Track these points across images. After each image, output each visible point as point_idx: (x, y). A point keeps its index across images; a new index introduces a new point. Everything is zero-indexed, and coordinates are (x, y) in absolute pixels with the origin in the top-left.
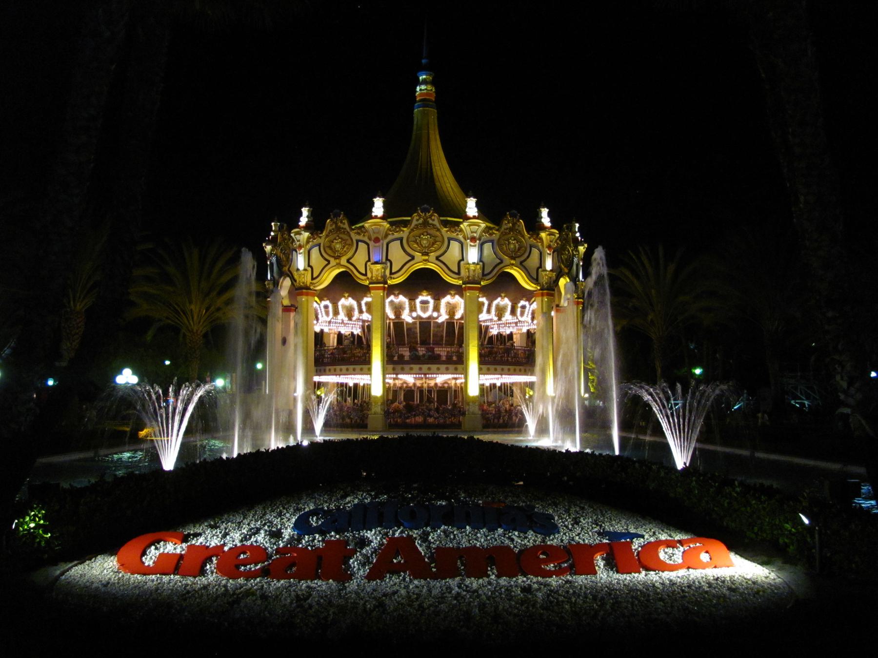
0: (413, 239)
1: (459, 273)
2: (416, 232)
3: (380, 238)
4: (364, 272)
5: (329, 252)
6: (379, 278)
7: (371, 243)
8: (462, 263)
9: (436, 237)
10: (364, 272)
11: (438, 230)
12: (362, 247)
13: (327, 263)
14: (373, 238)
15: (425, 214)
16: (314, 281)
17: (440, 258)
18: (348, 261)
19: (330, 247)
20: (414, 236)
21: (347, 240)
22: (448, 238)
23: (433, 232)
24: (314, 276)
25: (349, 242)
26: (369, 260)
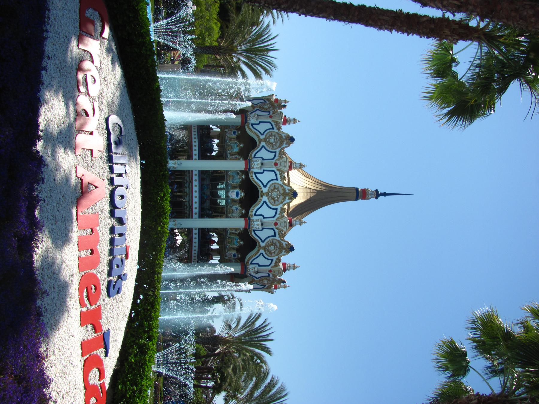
0: (277, 187)
1: (255, 215)
2: (281, 189)
3: (278, 166)
4: (256, 156)
5: (268, 135)
6: (253, 166)
7: (274, 161)
8: (261, 217)
9: (278, 200)
10: (256, 156)
11: (282, 203)
12: (272, 155)
13: (262, 133)
14: (277, 162)
15: (292, 194)
16: (250, 126)
18: (263, 146)
19: (271, 135)
20: (278, 187)
21: (276, 146)
23: (281, 199)
24: (254, 126)
25: (275, 147)
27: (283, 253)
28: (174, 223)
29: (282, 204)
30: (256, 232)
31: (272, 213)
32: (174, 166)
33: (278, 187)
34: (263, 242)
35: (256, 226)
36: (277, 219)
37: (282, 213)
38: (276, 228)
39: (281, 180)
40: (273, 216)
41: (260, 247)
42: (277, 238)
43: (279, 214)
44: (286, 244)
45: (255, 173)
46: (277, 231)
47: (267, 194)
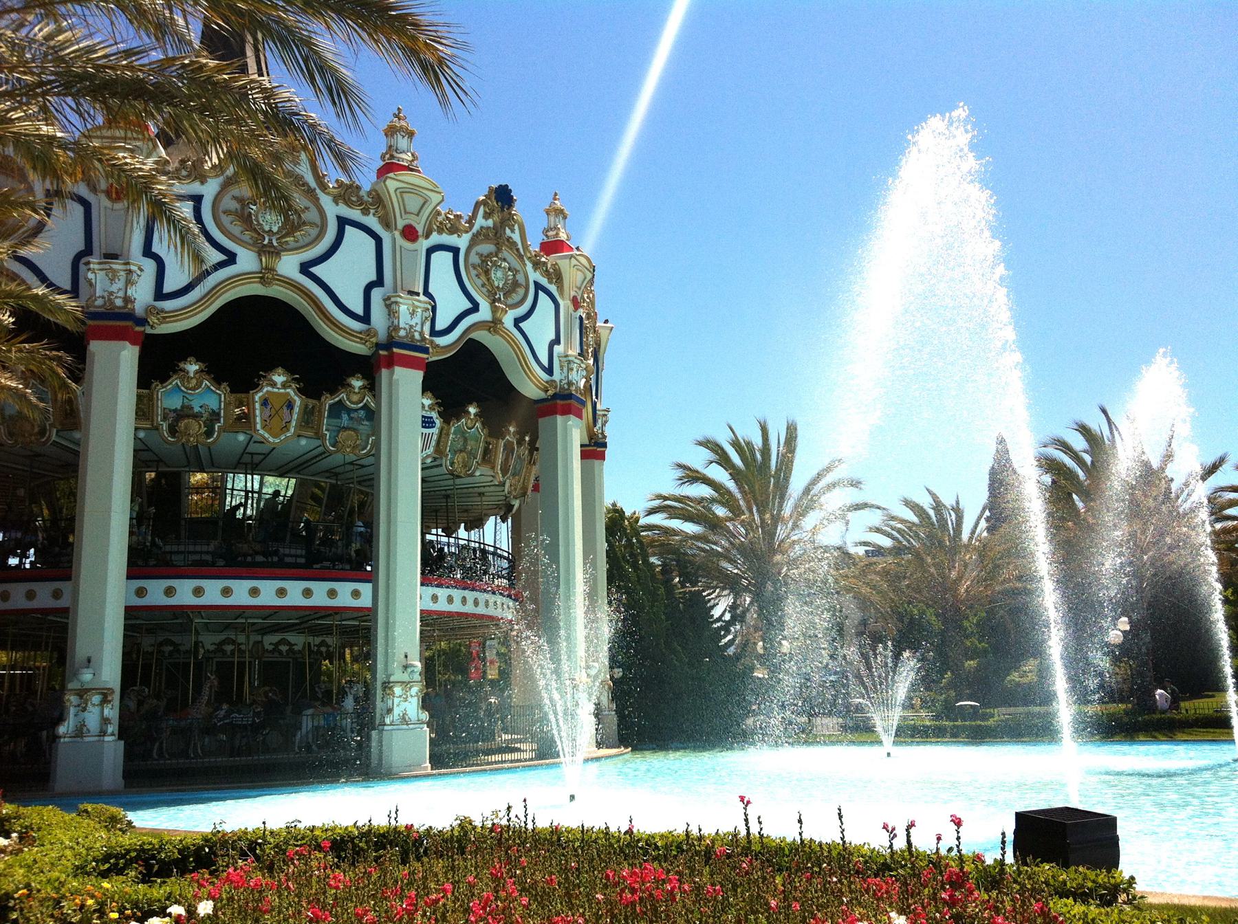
0: (234, 205)
1: (366, 318)
6: (119, 302)
8: (376, 294)
11: (310, 193)
17: (314, 270)
22: (337, 216)
26: (88, 251)
27: (516, 237)
28: (398, 690)
29: (318, 191)
30: (440, 326)
31: (357, 246)
32: (96, 699)
33: (234, 198)
34: (475, 308)
35: (417, 320)
36: (387, 224)
37: (360, 199)
38: (427, 237)
39: (203, 179)
40: (373, 242)
41: (494, 325)
42: (462, 242)
43: (365, 212)
44: (487, 216)
45: (160, 295)
46: (435, 239)
47: (268, 251)
